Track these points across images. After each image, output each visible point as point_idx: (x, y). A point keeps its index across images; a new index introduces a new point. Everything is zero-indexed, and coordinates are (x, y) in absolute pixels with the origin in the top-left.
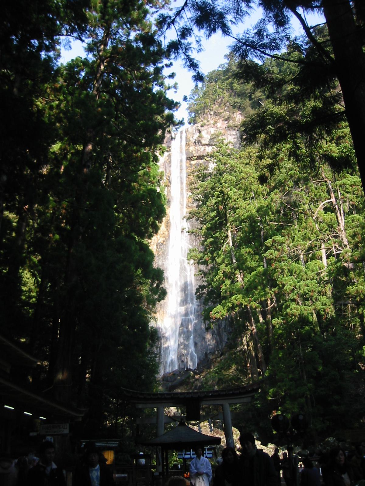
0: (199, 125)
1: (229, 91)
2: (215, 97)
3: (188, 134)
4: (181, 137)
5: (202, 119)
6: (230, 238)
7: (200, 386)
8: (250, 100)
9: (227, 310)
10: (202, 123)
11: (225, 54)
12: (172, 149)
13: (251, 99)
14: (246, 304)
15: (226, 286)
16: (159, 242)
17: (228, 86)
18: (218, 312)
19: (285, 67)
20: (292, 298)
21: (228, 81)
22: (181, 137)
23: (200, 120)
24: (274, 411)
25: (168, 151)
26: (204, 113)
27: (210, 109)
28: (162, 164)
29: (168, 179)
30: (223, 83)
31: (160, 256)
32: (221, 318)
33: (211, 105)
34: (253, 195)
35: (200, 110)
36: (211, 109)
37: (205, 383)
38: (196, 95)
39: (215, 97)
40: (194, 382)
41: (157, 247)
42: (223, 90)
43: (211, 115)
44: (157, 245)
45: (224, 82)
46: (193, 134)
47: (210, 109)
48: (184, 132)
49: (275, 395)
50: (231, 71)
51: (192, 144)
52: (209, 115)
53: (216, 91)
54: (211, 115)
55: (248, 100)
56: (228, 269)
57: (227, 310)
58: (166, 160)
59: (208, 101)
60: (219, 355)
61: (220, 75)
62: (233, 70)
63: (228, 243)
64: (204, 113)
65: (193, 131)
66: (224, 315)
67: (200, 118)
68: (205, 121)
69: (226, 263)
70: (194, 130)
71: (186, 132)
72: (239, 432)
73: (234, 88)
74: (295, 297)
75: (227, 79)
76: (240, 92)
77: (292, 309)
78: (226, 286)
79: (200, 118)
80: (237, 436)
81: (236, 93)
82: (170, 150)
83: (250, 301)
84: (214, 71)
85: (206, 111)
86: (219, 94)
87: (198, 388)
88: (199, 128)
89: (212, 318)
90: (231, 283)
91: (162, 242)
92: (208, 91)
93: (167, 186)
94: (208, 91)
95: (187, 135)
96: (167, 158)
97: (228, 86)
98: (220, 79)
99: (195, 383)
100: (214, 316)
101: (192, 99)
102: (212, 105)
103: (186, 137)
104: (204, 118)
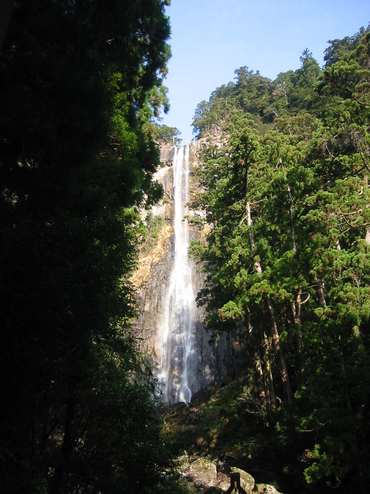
0: (204, 139)
1: (238, 106)
2: (223, 111)
3: (192, 148)
4: (184, 152)
5: (208, 134)
6: (249, 215)
7: (196, 419)
8: (261, 116)
9: (242, 307)
10: (208, 137)
11: (236, 68)
12: (174, 163)
13: (262, 114)
14: (272, 292)
15: (241, 276)
16: (154, 261)
17: (237, 101)
18: (229, 310)
19: (301, 80)
20: (346, 277)
21: (237, 97)
22: (184, 152)
23: (206, 134)
24: (306, 450)
25: (169, 166)
26: (211, 127)
27: (217, 124)
28: (162, 179)
29: (168, 195)
30: (233, 98)
31: (154, 277)
32: (234, 318)
33: (218, 119)
34: (281, 162)
35: (206, 124)
36: (219, 123)
37: (203, 417)
38: (202, 111)
39: (223, 111)
40: (188, 415)
41: (151, 267)
42: (232, 105)
43: (218, 130)
44: (151, 265)
45: (233, 97)
47: (217, 124)
48: (188, 146)
49: (310, 425)
50: (241, 86)
51: (196, 159)
52: (216, 130)
53: (224, 106)
54: (218, 130)
55: (258, 116)
56: (245, 252)
57: (242, 307)
58: (167, 174)
59: (216, 116)
60: (219, 386)
61: (229, 90)
62: (243, 84)
63: (246, 222)
64: (211, 127)
65: (198, 145)
66: (238, 313)
67: (205, 132)
68: (212, 136)
69: (243, 244)
70: (199, 145)
71: (190, 146)
72: (254, 480)
73: (245, 102)
74: (351, 274)
75: (237, 94)
76: (250, 107)
77: (346, 292)
78: (241, 276)
79: (205, 132)
80: (251, 485)
81: (246, 109)
82: (172, 164)
83: (278, 289)
84: (223, 86)
85: (213, 125)
86: (227, 109)
87: (193, 421)
88: (205, 142)
89: (221, 317)
90: (249, 273)
91: (157, 262)
92: (216, 105)
93: (166, 202)
94: (216, 105)
95: (190, 149)
96: (168, 172)
97: (237, 101)
98: (229, 94)
99: (190, 415)
100: (223, 315)
101: (198, 113)
102: (220, 120)
103: (190, 152)
104: (210, 133)
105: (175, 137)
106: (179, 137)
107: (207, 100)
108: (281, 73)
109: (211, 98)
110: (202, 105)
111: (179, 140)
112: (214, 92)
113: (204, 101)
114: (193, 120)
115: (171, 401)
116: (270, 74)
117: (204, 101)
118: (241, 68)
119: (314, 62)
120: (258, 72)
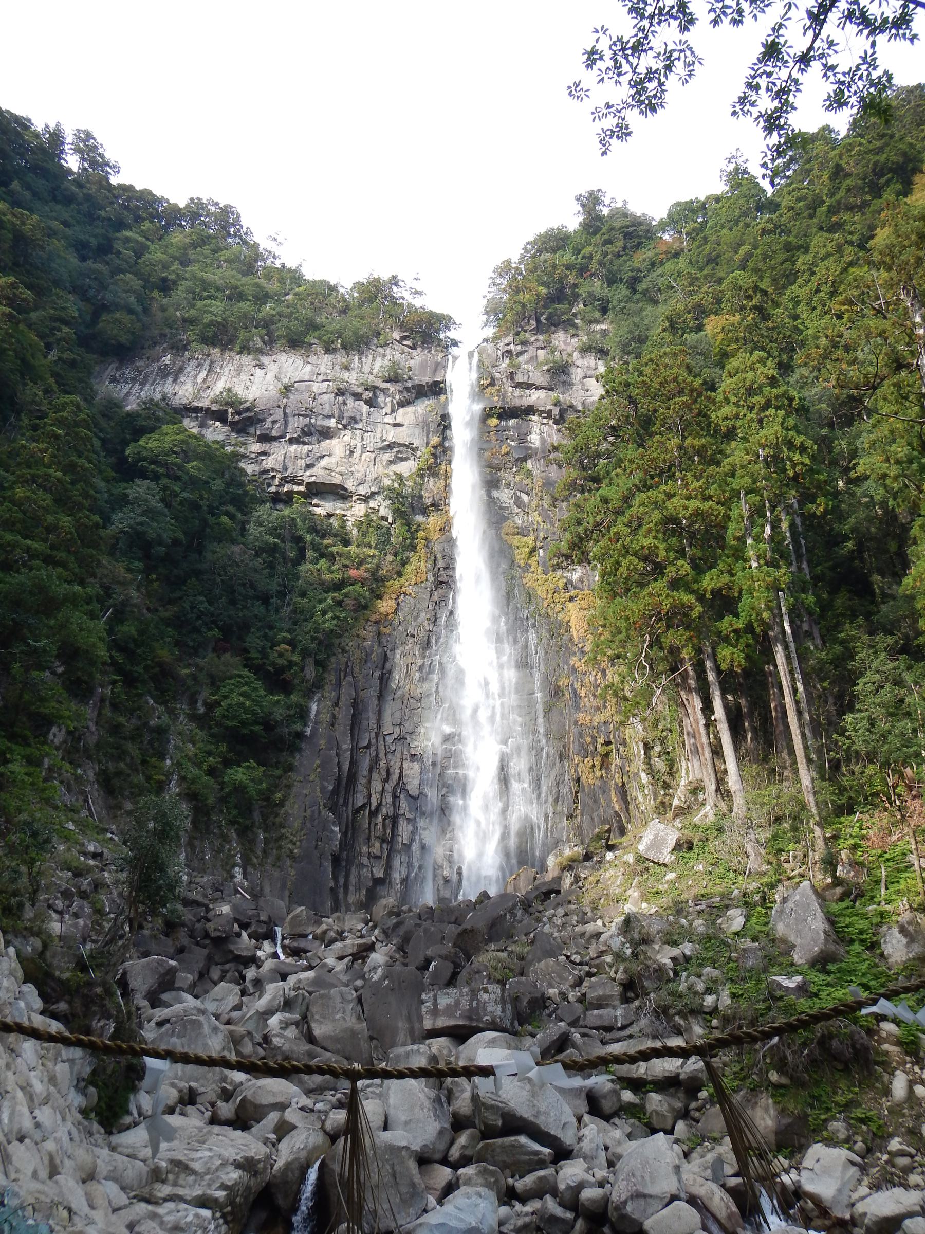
48: (476, 354)
105: (448, 334)
106: (452, 334)
107: (515, 258)
108: (678, 204)
109: (522, 256)
110: (505, 269)
111: (455, 343)
112: (528, 243)
113: (509, 262)
114: (485, 302)
115: (441, 888)
116: (652, 205)
117: (509, 262)
118: (591, 193)
119: (753, 181)
120: (625, 202)
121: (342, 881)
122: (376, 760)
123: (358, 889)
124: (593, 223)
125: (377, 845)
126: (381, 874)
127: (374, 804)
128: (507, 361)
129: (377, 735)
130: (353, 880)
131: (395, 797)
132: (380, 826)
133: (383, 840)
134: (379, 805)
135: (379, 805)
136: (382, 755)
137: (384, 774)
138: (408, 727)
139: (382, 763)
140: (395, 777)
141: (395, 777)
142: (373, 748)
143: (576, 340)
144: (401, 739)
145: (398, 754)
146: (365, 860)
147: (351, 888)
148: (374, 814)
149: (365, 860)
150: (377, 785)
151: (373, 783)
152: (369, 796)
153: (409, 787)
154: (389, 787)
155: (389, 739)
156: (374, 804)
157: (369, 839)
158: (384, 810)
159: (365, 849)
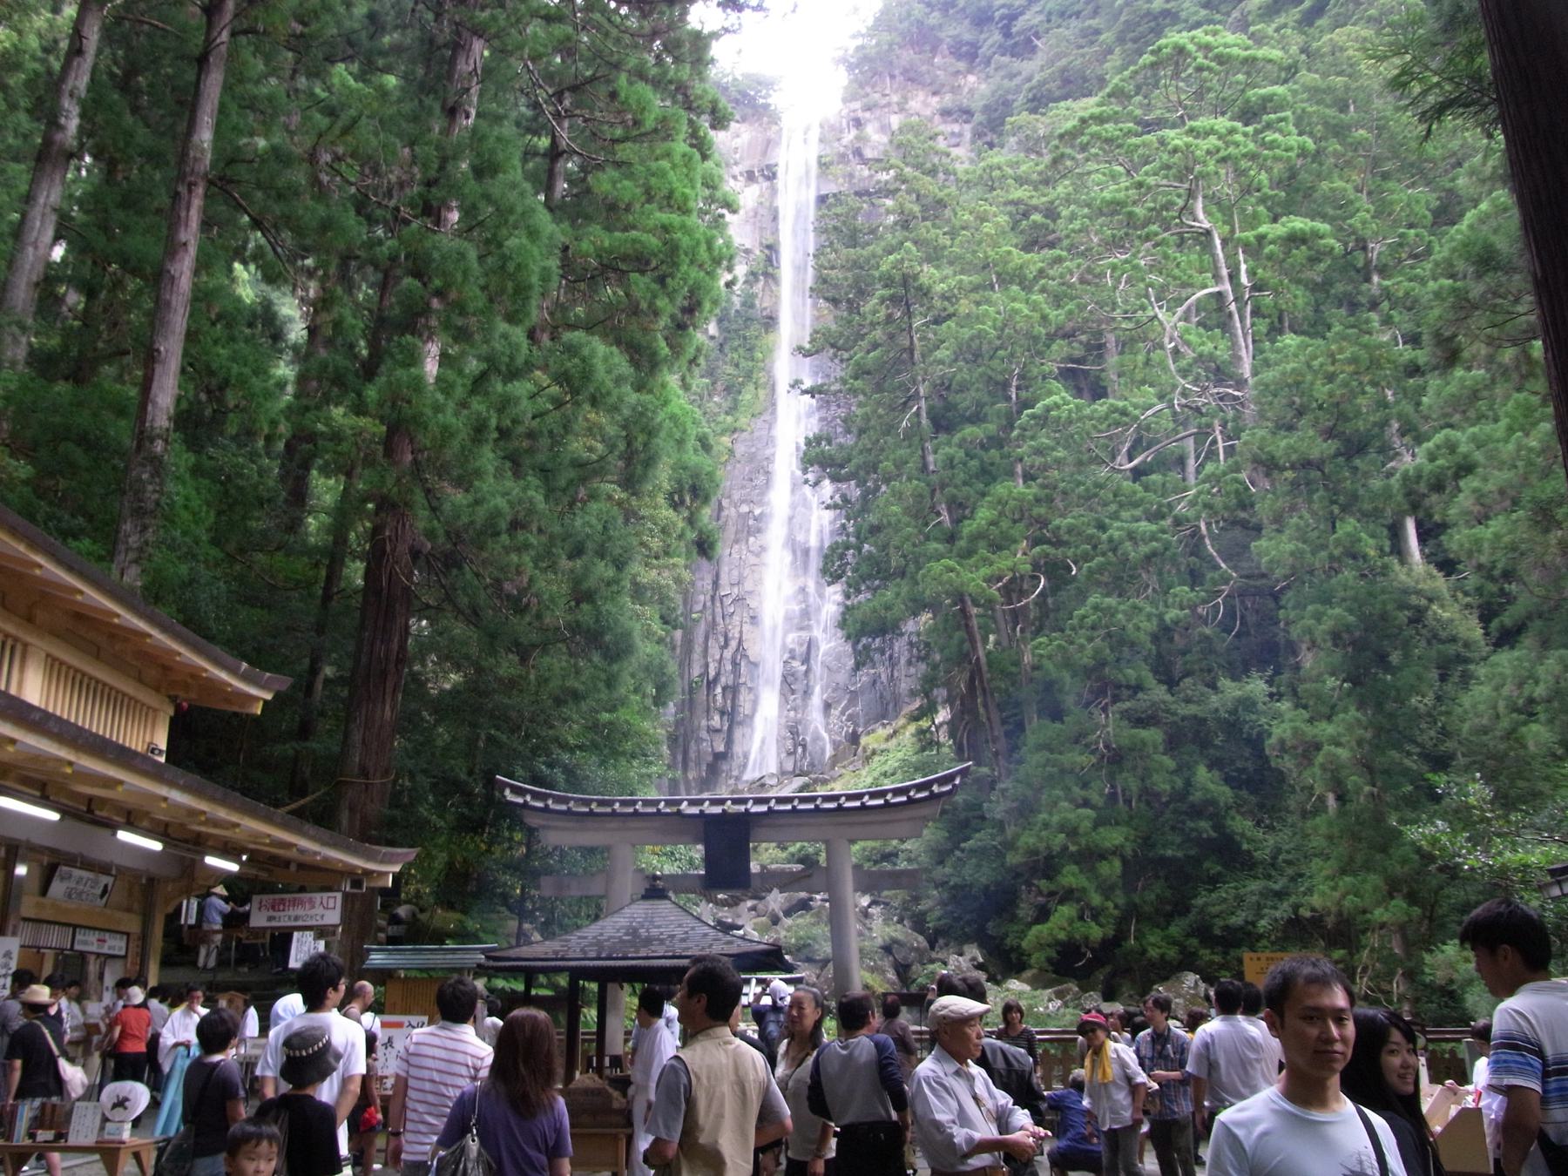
46: (841, 131)
121: (680, 758)
122: (713, 624)
123: (698, 764)
124: (851, 68)
125: (717, 718)
126: (721, 748)
127: (712, 673)
128: (854, 132)
129: (713, 598)
130: (692, 755)
131: (735, 664)
132: (719, 698)
133: (722, 713)
134: (718, 674)
135: (718, 674)
136: (719, 619)
137: (722, 639)
138: (748, 586)
139: (721, 627)
140: (733, 644)
141: (733, 644)
142: (709, 612)
143: (936, 99)
144: (739, 600)
145: (736, 618)
146: (704, 734)
147: (692, 764)
148: (711, 684)
149: (704, 734)
150: (714, 652)
151: (710, 651)
152: (707, 666)
153: (749, 653)
154: (728, 654)
155: (728, 601)
156: (712, 673)
157: (708, 711)
158: (723, 680)
159: (704, 723)
